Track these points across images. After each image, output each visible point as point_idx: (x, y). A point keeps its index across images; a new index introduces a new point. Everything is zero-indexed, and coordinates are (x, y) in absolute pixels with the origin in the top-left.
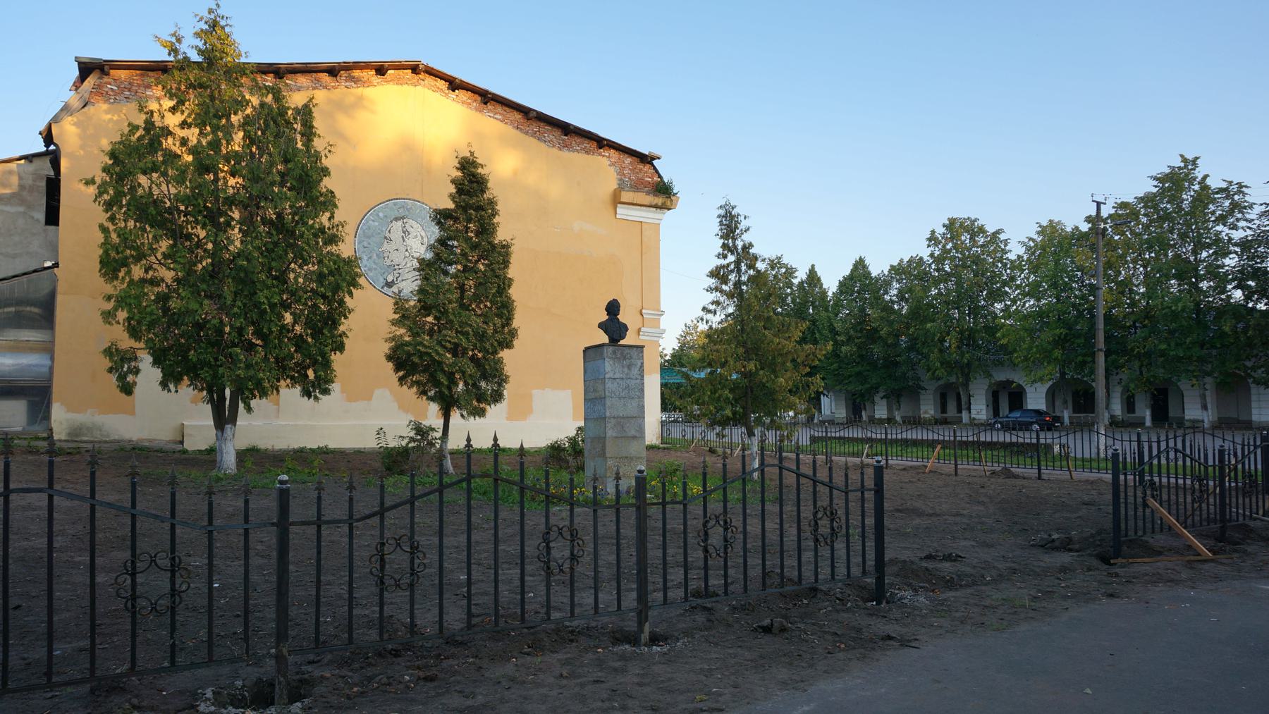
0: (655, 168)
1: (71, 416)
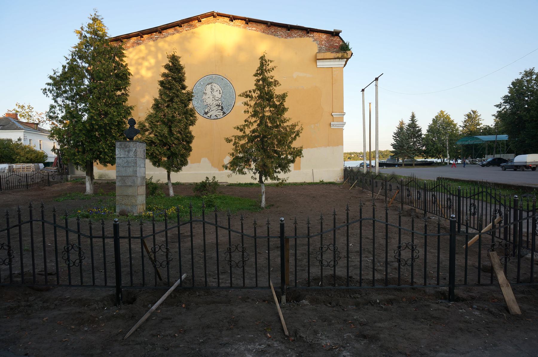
0: (340, 38)
1: (99, 171)
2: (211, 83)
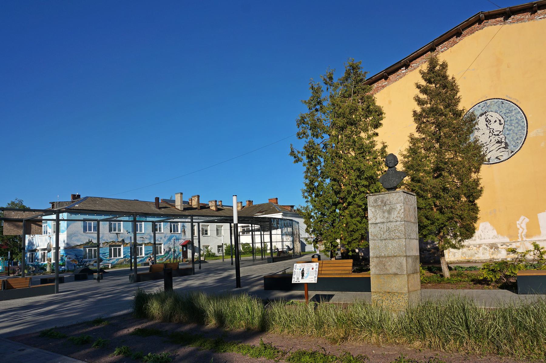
2: (486, 112)
